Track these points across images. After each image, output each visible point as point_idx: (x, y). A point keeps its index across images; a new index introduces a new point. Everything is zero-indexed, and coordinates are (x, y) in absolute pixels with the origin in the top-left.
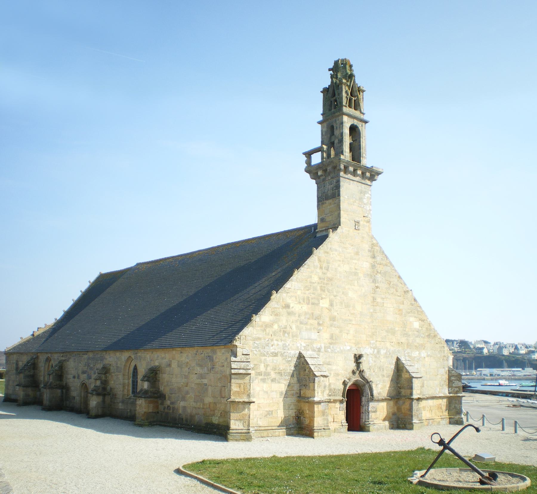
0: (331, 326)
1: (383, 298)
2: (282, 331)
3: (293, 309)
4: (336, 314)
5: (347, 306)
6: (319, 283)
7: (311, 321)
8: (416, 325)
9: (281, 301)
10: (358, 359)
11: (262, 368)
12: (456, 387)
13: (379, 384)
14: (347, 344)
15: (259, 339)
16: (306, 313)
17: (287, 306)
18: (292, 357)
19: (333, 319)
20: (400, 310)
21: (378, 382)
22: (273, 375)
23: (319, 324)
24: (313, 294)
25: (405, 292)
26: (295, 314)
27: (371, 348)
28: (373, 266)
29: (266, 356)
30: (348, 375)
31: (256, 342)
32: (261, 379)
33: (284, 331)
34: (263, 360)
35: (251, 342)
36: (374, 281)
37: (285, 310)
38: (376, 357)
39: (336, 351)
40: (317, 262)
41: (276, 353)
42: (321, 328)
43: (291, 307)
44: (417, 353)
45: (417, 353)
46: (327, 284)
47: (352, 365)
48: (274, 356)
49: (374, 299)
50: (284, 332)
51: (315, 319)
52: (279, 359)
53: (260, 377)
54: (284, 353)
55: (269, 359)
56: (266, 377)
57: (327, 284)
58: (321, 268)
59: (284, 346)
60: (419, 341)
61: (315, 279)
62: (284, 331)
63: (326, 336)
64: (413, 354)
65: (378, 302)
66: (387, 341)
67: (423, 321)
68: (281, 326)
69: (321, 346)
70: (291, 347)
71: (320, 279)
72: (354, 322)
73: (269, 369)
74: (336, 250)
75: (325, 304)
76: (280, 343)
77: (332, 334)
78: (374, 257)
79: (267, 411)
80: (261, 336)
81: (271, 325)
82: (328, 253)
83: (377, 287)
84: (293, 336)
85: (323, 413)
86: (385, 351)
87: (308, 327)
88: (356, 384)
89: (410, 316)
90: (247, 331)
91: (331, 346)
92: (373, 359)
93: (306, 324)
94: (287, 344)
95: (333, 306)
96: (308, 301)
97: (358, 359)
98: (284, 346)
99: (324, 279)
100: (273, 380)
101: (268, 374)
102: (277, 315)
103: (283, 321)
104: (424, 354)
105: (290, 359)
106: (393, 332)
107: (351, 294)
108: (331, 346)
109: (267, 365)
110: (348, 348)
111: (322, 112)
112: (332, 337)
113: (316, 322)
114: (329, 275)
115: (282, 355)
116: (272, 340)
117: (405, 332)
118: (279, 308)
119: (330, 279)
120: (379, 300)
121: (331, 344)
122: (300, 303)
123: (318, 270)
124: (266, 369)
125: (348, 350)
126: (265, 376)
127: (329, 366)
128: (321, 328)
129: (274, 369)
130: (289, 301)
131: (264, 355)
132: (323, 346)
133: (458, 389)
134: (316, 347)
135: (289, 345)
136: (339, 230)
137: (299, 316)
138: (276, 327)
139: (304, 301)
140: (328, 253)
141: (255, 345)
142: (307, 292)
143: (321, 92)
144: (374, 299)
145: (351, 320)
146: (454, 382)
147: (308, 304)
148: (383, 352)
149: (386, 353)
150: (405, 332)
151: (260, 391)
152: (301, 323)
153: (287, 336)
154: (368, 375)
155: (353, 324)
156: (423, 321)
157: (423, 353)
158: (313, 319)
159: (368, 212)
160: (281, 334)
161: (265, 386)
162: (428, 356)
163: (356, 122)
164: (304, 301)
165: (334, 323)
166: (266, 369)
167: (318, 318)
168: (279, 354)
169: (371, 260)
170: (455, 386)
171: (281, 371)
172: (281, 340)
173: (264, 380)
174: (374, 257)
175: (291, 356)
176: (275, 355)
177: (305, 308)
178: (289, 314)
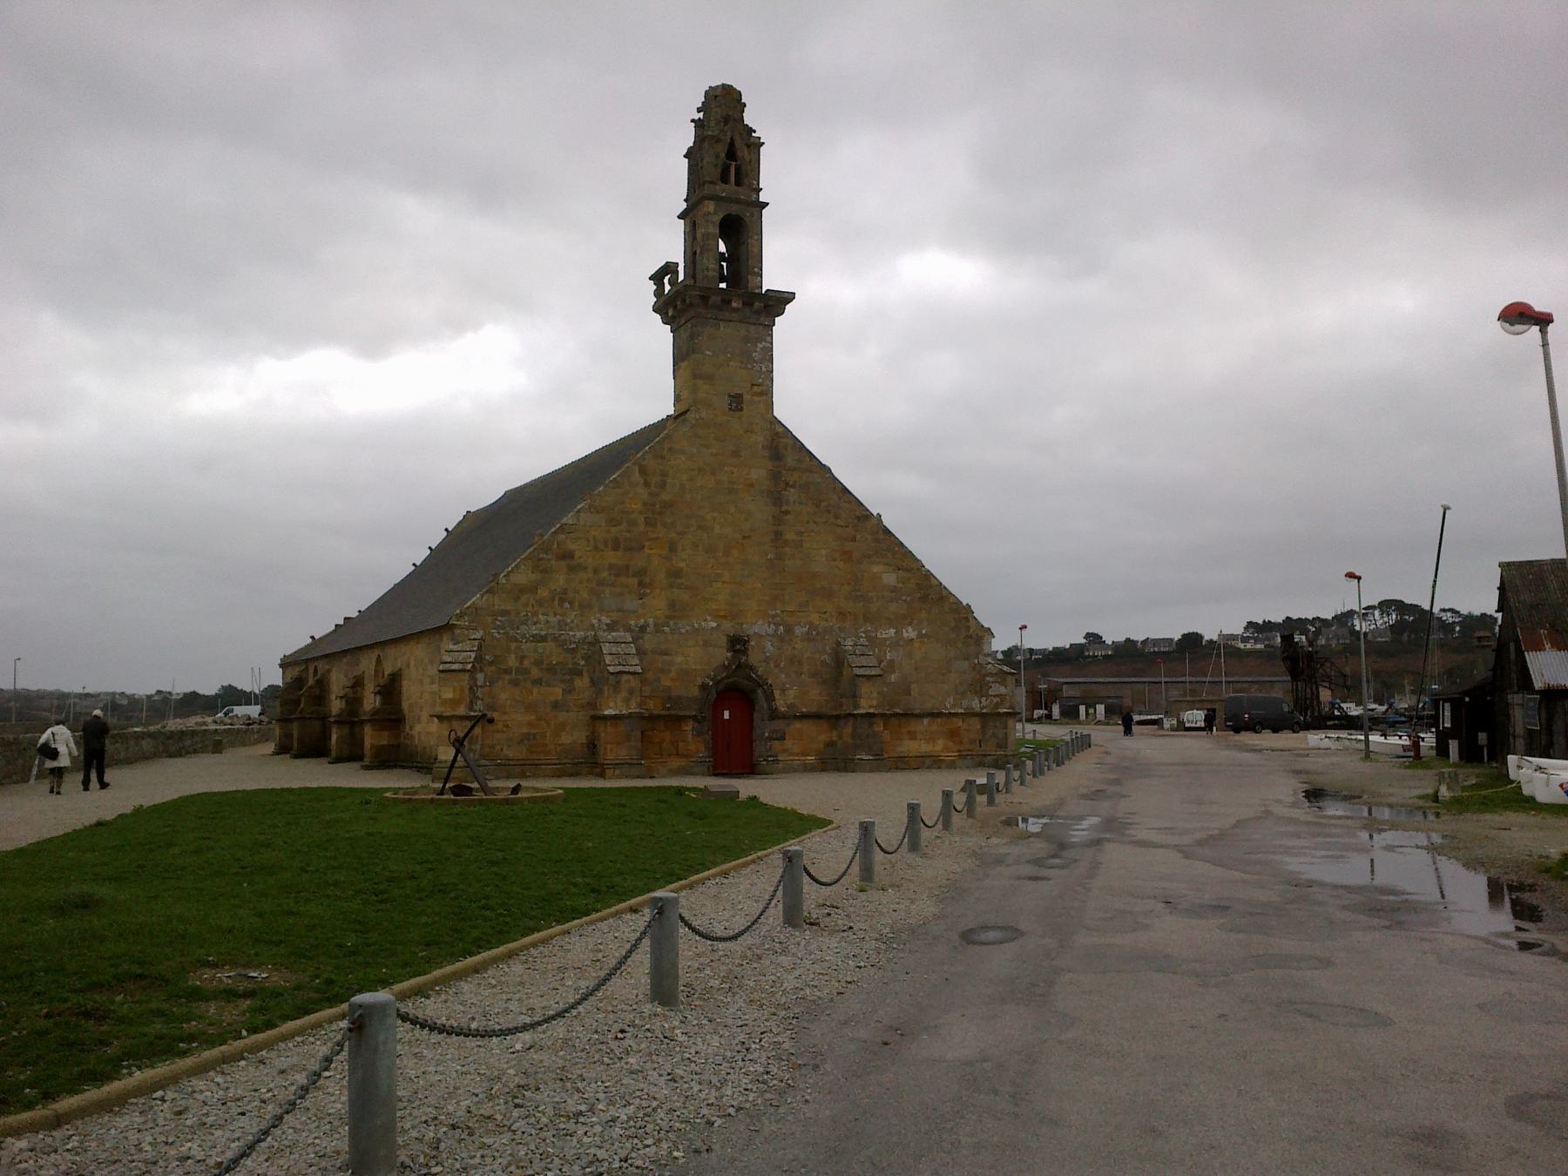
0: (671, 586)
1: (800, 533)
2: (557, 599)
3: (582, 560)
4: (682, 565)
6: (641, 512)
7: (623, 579)
8: (890, 579)
9: (555, 546)
10: (738, 644)
12: (995, 696)
13: (788, 689)
14: (709, 618)
15: (505, 613)
16: (611, 567)
18: (579, 642)
19: (675, 574)
20: (845, 553)
21: (788, 686)
22: (535, 673)
23: (641, 584)
24: (629, 531)
25: (858, 518)
26: (586, 568)
27: (770, 623)
28: (775, 476)
29: (521, 642)
30: (712, 673)
31: (499, 618)
32: (510, 682)
34: (513, 648)
35: (490, 619)
37: (563, 563)
38: (781, 639)
39: (683, 631)
40: (637, 475)
41: (541, 636)
42: (648, 591)
43: (576, 557)
44: (892, 631)
45: (892, 631)
46: (660, 513)
48: (539, 642)
49: (778, 534)
50: (562, 601)
51: (633, 576)
52: (551, 645)
53: (507, 677)
54: (560, 636)
56: (520, 677)
57: (660, 513)
58: (647, 484)
59: (562, 625)
62: (560, 598)
63: (657, 604)
64: (878, 634)
65: (785, 540)
66: (811, 609)
67: (909, 570)
68: (555, 590)
69: (645, 622)
70: (577, 626)
71: (644, 504)
72: (726, 579)
73: (526, 663)
74: (683, 452)
76: (553, 620)
77: (674, 601)
79: (523, 734)
80: (508, 608)
81: (533, 589)
82: (663, 457)
83: (787, 513)
84: (581, 606)
86: (805, 629)
87: (618, 590)
89: (873, 563)
91: (671, 623)
92: (776, 644)
93: (613, 585)
94: (569, 621)
95: (676, 552)
97: (738, 644)
98: (562, 625)
99: (654, 505)
100: (538, 682)
101: (526, 671)
102: (544, 571)
103: (560, 580)
104: (909, 633)
105: (573, 646)
108: (671, 623)
109: (523, 658)
110: (714, 625)
111: (685, 197)
112: (672, 605)
113: (635, 581)
114: (665, 497)
115: (555, 639)
116: (535, 614)
117: (859, 593)
118: (548, 560)
120: (790, 536)
121: (670, 617)
122: (596, 548)
123: (641, 490)
124: (521, 663)
125: (712, 628)
127: (666, 657)
128: (648, 591)
129: (538, 663)
130: (573, 547)
131: (516, 640)
132: (651, 621)
133: (998, 699)
134: (636, 626)
135: (572, 621)
137: (596, 571)
138: (543, 593)
139: (606, 546)
140: (663, 457)
141: (497, 622)
142: (613, 529)
143: (685, 156)
144: (778, 534)
145: (719, 575)
146: (991, 687)
147: (616, 548)
148: (799, 631)
149: (807, 633)
150: (859, 593)
151: (506, 700)
152: (601, 583)
153: (569, 606)
155: (724, 582)
156: (909, 570)
157: (907, 631)
158: (628, 576)
159: (763, 376)
160: (556, 602)
162: (920, 636)
163: (734, 209)
164: (606, 546)
165: (678, 581)
166: (521, 663)
167: (641, 573)
168: (549, 639)
170: (993, 694)
171: (554, 665)
172: (555, 615)
173: (515, 683)
175: (577, 641)
176: (543, 639)
178: (572, 569)
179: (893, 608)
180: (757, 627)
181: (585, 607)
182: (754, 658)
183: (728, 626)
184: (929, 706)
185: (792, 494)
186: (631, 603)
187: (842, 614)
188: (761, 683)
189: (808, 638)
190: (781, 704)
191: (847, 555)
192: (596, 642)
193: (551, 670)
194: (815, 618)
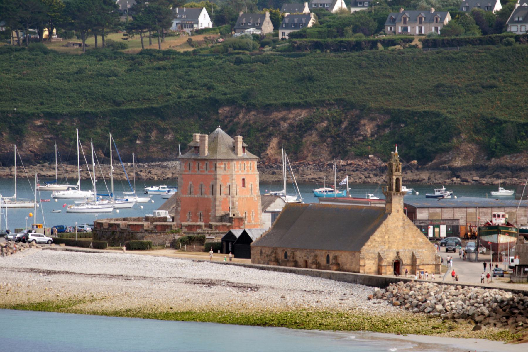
5: (394, 237)
8: (421, 240)
10: (398, 253)
11: (368, 257)
17: (375, 240)
19: (389, 242)
28: (404, 223)
33: (374, 246)
36: (404, 228)
47: (396, 255)
55: (370, 254)
60: (422, 246)
61: (383, 230)
63: (387, 247)
75: (386, 237)
78: (404, 220)
81: (370, 245)
85: (385, 269)
88: (397, 260)
90: (364, 247)
96: (381, 237)
97: (398, 253)
103: (374, 244)
104: (424, 250)
106: (411, 244)
107: (395, 233)
119: (388, 230)
126: (369, 259)
136: (391, 214)
144: (404, 234)
154: (401, 257)
161: (369, 262)
163: (398, 177)
167: (384, 242)
169: (403, 222)
174: (404, 220)
177: (380, 239)
179: (422, 246)
180: (401, 250)
181: (377, 248)
182: (400, 255)
183: (397, 250)
184: (427, 263)
185: (406, 226)
186: (383, 247)
187: (413, 247)
188: (401, 260)
189: (408, 251)
190: (404, 263)
191: (414, 237)
192: (379, 253)
193: (373, 258)
194: (409, 248)
